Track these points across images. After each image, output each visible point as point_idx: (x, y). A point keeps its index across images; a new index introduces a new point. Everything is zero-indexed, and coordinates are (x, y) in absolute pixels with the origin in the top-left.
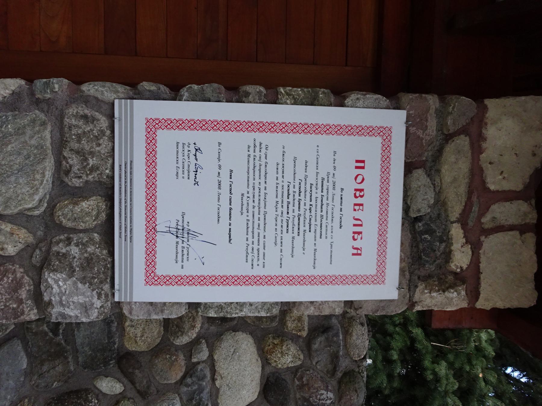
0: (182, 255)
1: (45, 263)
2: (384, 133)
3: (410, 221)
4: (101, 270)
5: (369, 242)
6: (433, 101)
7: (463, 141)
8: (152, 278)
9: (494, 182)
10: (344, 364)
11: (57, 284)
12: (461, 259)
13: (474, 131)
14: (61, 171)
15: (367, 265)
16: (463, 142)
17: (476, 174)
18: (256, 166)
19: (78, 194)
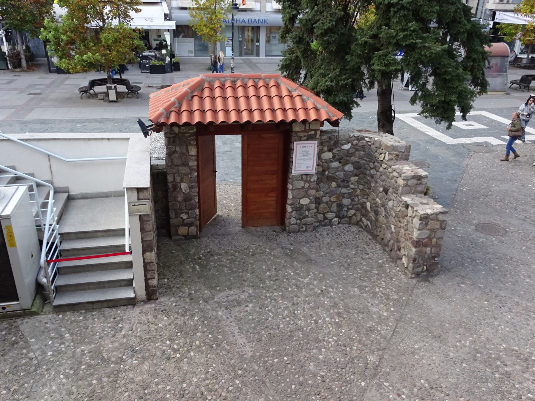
0: (310, 167)
1: (310, 182)
2: (297, 144)
3: (307, 140)
4: (311, 176)
5: (310, 145)
6: (293, 138)
7: (298, 134)
8: (313, 170)
9: (303, 129)
10: (328, 139)
11: (312, 180)
12: (313, 132)
13: (297, 132)
14: (300, 180)
15: (313, 145)
16: (298, 134)
17: (302, 131)
18: (300, 159)
19: (302, 178)
